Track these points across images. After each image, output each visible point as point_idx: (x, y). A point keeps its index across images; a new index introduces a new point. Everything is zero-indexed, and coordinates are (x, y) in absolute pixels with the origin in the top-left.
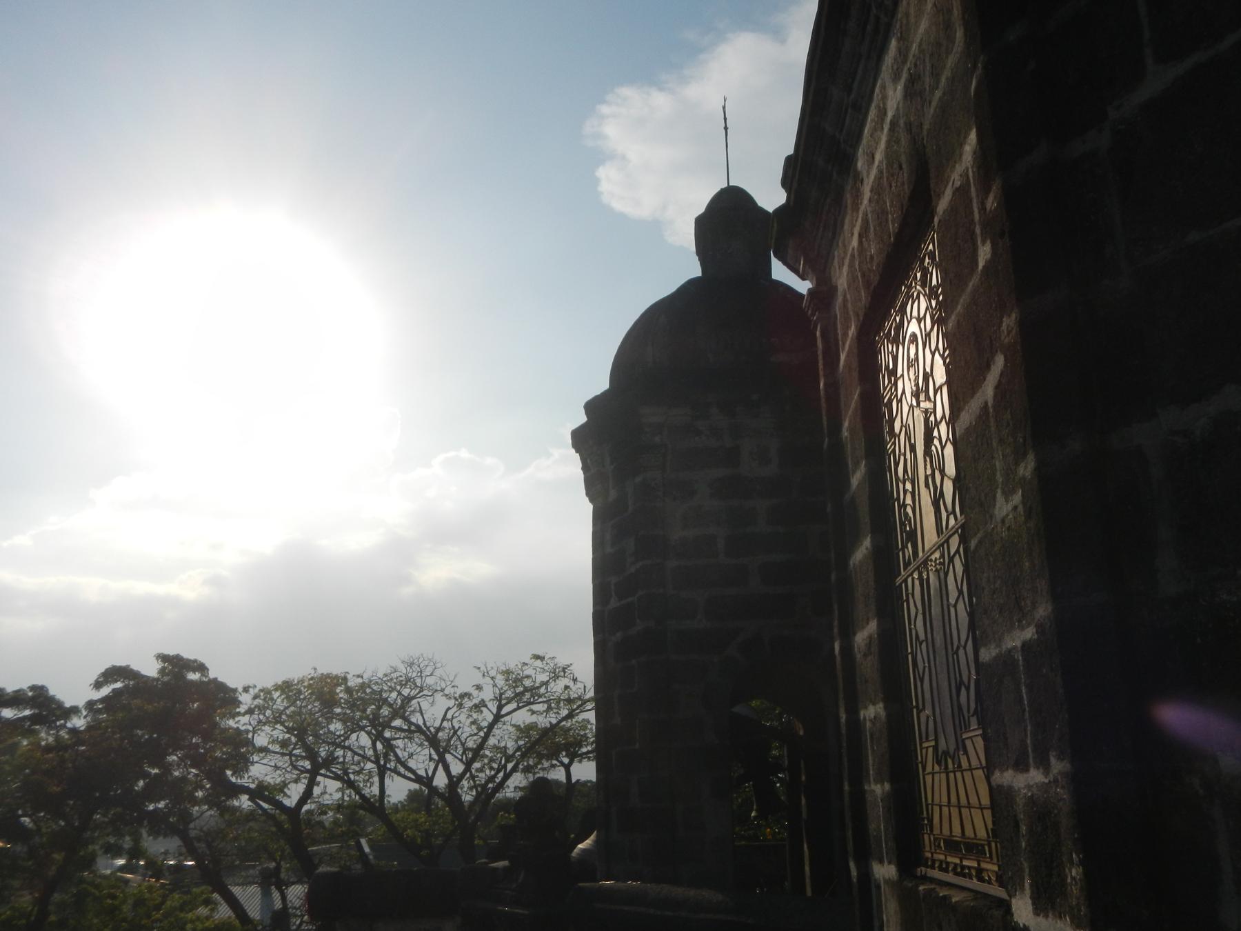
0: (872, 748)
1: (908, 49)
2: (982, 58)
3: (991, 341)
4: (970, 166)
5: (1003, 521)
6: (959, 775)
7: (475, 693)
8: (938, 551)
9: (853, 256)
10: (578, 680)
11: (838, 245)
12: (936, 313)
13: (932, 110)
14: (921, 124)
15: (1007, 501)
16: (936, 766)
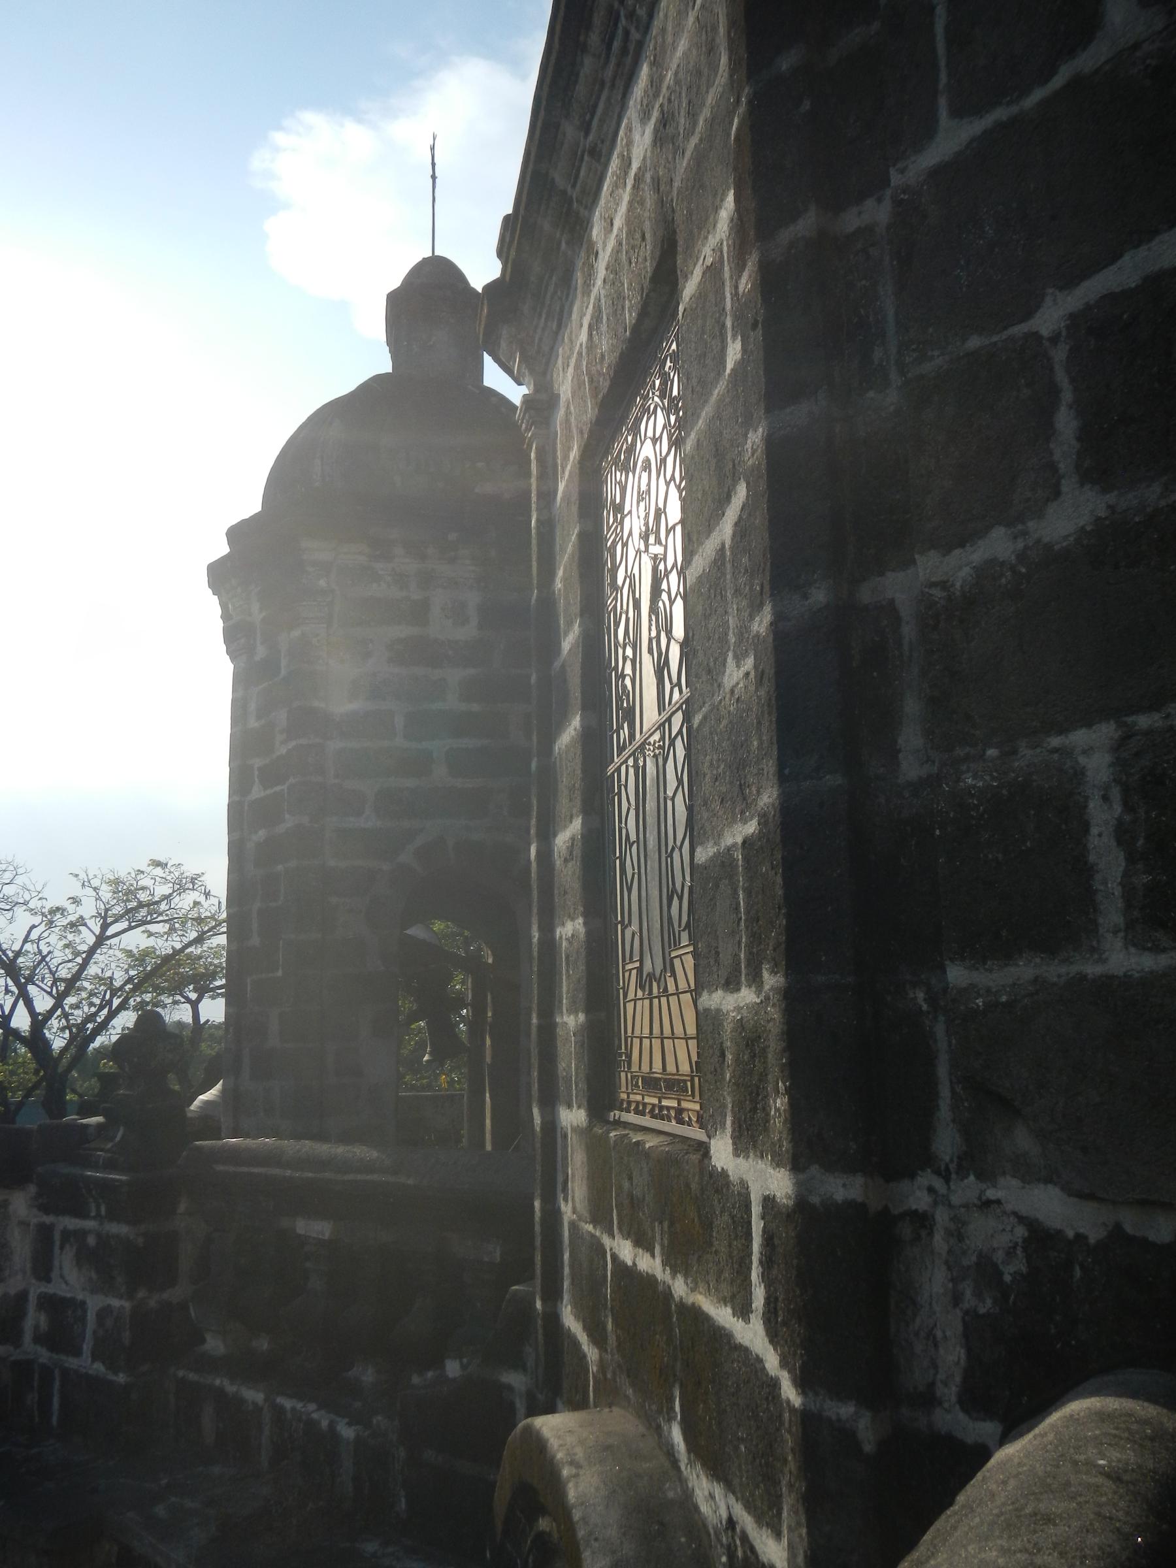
0: (567, 971)
1: (661, 78)
2: (746, 90)
3: (734, 465)
4: (725, 238)
5: (732, 692)
6: (664, 1000)
7: (71, 908)
8: (658, 731)
9: (580, 354)
10: (211, 893)
12: (675, 432)
14: (671, 180)
15: (738, 666)
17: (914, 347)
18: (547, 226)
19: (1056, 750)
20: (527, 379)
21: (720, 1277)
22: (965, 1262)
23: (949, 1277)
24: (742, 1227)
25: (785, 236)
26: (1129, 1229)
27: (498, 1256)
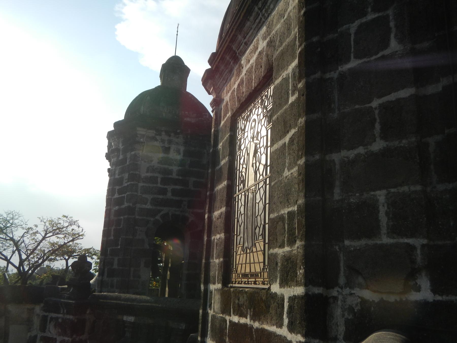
0: (216, 248)
1: (271, 32)
2: (304, 43)
3: (290, 125)
5: (286, 177)
6: (251, 254)
7: (34, 228)
9: (234, 90)
10: (80, 226)
13: (278, 52)
14: (273, 56)
15: (289, 171)
16: (242, 252)
17: (343, 105)
18: (228, 58)
19: (372, 195)
20: (214, 94)
21: (272, 319)
22: (346, 307)
24: (281, 305)
25: (313, 77)
26: (385, 299)
27: (184, 327)
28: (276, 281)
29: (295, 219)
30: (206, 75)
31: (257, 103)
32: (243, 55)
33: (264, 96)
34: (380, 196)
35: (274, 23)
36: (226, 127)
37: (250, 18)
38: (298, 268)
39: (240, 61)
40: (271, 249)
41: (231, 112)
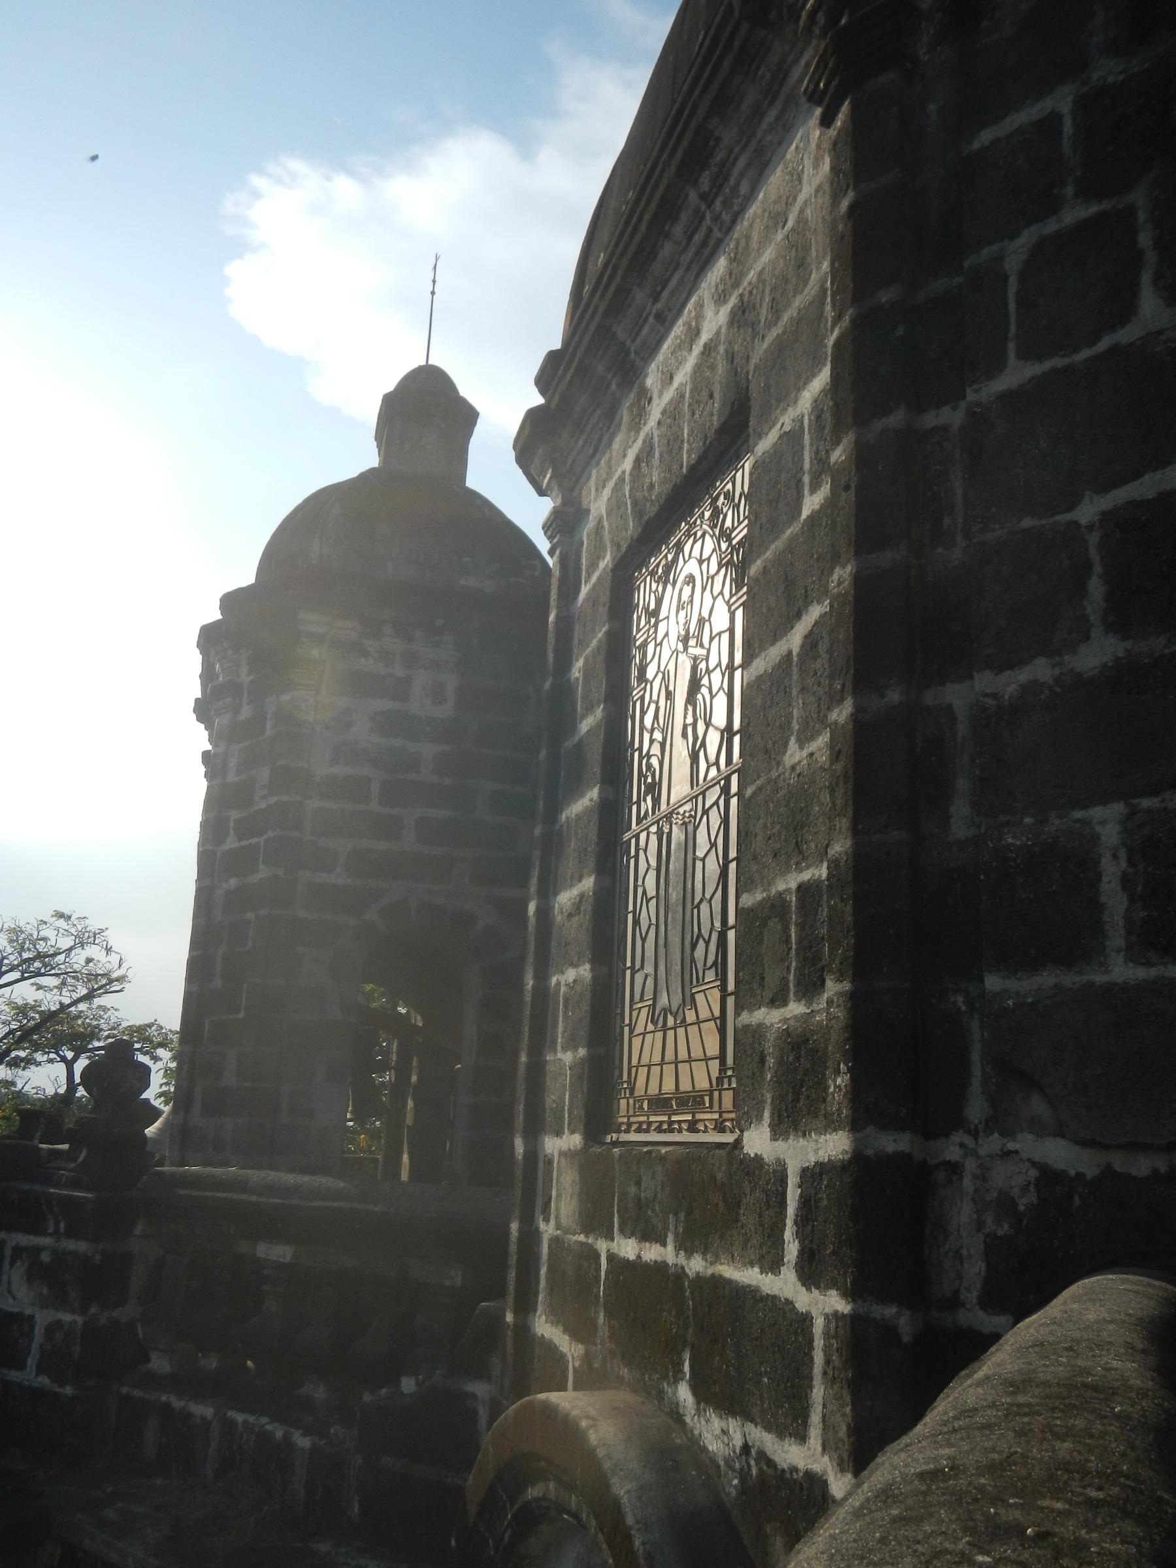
0: (565, 1013)
1: (742, 275)
2: (851, 311)
3: (806, 591)
5: (793, 768)
8: (690, 803)
9: (622, 480)
10: (113, 949)
11: (598, 463)
12: (726, 556)
13: (765, 345)
14: (748, 357)
15: (801, 748)
17: (979, 520)
18: (600, 368)
21: (747, 1245)
22: (988, 1198)
23: (975, 1210)
24: (776, 1198)
25: (879, 425)
26: (1117, 1167)
27: (459, 1281)
28: (760, 1118)
29: (820, 909)
30: (528, 426)
31: (698, 522)
32: (650, 356)
33: (722, 497)
34: (1102, 823)
35: (754, 244)
36: (595, 603)
37: (673, 230)
38: (830, 1070)
39: (641, 378)
40: (743, 1009)
41: (614, 554)
